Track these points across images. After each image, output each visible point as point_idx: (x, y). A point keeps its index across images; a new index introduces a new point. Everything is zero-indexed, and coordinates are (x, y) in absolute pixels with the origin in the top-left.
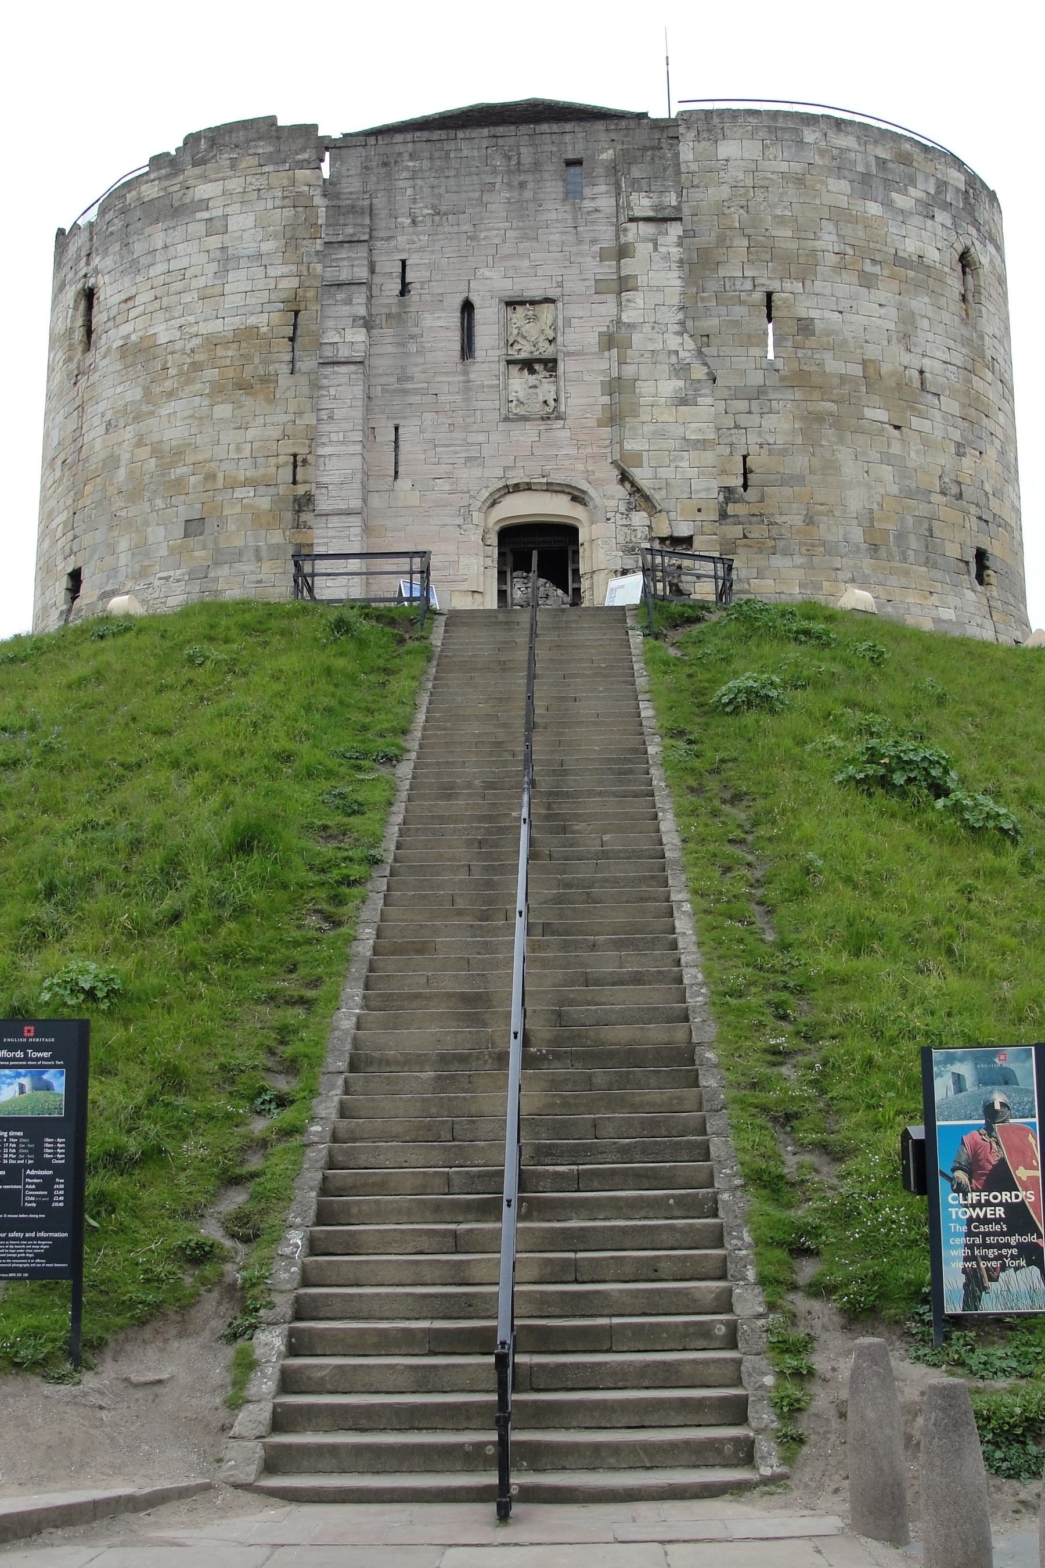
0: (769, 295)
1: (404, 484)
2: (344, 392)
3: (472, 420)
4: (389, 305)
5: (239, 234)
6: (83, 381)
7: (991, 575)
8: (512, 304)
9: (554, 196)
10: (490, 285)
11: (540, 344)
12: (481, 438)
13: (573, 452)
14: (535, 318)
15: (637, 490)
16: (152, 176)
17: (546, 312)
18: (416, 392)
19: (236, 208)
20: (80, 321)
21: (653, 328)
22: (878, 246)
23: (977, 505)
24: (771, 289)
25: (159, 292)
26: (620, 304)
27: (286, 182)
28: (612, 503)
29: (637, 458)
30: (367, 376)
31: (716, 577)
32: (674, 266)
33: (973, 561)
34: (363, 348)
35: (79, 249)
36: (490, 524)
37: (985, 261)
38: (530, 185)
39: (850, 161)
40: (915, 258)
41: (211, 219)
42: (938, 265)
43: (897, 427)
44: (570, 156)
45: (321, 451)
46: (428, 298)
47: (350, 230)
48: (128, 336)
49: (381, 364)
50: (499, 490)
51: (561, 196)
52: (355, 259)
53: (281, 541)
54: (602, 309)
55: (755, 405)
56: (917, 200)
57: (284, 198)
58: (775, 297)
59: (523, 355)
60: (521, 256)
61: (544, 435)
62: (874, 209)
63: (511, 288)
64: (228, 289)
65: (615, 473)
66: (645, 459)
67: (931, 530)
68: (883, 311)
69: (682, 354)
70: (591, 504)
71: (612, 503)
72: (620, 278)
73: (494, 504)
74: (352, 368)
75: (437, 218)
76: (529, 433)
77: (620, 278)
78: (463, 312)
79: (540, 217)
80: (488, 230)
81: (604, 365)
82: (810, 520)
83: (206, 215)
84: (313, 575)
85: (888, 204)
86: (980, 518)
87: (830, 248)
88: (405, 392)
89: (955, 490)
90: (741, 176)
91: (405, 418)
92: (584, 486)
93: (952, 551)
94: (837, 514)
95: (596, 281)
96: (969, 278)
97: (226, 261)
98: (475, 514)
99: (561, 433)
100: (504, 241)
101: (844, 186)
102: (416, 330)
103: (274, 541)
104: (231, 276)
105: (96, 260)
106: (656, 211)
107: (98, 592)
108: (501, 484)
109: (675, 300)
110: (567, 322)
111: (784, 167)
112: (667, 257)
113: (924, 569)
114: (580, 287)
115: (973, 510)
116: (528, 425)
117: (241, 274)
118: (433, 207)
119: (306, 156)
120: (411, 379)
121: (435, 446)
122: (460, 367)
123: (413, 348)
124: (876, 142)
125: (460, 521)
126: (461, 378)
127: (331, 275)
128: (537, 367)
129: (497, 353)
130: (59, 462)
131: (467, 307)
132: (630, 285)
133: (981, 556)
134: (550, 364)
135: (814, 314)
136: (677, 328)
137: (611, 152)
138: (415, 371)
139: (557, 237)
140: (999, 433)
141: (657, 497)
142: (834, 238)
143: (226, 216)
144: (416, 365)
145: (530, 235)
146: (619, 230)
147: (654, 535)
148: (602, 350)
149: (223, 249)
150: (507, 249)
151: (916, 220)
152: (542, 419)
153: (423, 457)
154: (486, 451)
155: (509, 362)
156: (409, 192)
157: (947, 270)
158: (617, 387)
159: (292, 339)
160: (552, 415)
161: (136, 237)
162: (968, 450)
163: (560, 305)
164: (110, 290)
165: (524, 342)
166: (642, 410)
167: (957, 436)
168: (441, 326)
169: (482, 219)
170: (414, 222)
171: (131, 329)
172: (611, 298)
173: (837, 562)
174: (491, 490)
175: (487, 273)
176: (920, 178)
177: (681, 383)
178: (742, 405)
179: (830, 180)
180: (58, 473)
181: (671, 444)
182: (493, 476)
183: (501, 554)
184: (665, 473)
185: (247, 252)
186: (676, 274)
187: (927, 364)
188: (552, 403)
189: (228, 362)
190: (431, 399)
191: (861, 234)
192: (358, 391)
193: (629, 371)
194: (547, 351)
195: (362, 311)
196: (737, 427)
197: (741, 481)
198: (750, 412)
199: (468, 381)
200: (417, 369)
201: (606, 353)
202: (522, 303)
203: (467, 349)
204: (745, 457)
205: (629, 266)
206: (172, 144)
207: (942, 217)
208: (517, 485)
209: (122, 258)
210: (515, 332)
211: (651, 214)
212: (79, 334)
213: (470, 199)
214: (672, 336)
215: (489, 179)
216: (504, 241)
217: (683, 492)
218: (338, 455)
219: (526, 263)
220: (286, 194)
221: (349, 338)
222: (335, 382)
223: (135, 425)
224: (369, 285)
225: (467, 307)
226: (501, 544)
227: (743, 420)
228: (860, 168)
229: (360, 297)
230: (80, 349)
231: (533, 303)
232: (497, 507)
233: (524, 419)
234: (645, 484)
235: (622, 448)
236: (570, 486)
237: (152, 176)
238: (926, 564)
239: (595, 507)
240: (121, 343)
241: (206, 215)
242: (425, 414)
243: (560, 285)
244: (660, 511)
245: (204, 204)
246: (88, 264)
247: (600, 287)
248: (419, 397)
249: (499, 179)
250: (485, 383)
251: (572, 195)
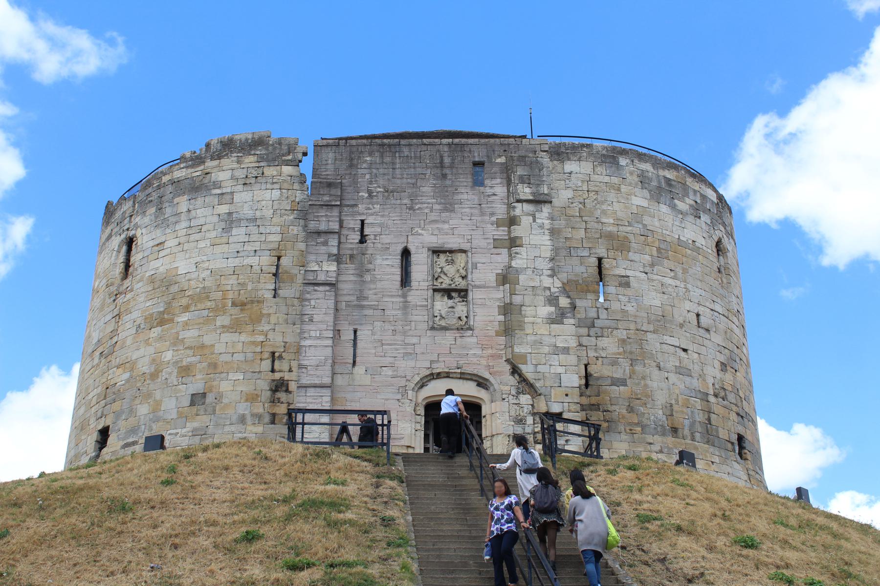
0: (600, 260)
1: (359, 370)
2: (321, 305)
3: (408, 328)
4: (352, 249)
5: (240, 205)
6: (121, 299)
8: (436, 252)
9: (465, 184)
11: (456, 280)
12: (415, 340)
13: (479, 352)
14: (452, 262)
15: (523, 380)
16: (182, 166)
17: (460, 259)
18: (370, 307)
19: (240, 187)
20: (122, 258)
21: (533, 272)
22: (668, 233)
23: (736, 405)
24: (601, 255)
25: (182, 240)
26: (510, 255)
27: (275, 173)
28: (507, 388)
29: (523, 358)
30: (336, 295)
31: (589, 437)
32: (547, 232)
33: (736, 442)
34: (335, 275)
35: (124, 212)
36: (420, 400)
37: (730, 248)
38: (449, 177)
39: (648, 179)
40: (690, 242)
41: (223, 194)
42: (705, 248)
43: (685, 350)
44: (477, 159)
45: (303, 343)
46: (379, 246)
47: (326, 198)
48: (157, 269)
49: (346, 287)
50: (426, 376)
51: (470, 184)
52: (331, 216)
53: (261, 410)
54: (498, 258)
55: (593, 331)
56: (691, 206)
57: (273, 183)
58: (605, 261)
59: (444, 286)
60: (444, 222)
61: (459, 340)
62: (664, 208)
63: (434, 241)
64: (231, 240)
65: (508, 368)
66: (529, 359)
67: (709, 419)
68: (672, 274)
69: (553, 290)
70: (491, 389)
71: (507, 388)
72: (510, 239)
73: (422, 387)
74: (327, 288)
75: (386, 194)
77: (510, 239)
78: (402, 256)
79: (456, 197)
80: (422, 203)
81: (499, 294)
82: (631, 409)
83: (218, 191)
84: (303, 424)
85: (673, 207)
86: (738, 414)
87: (638, 232)
88: (362, 307)
89: (722, 394)
90: (580, 184)
91: (361, 324)
92: (486, 375)
94: (648, 406)
95: (494, 240)
96: (721, 258)
97: (230, 221)
98: (410, 392)
99: (470, 340)
100: (431, 211)
101: (646, 193)
102: (371, 266)
103: (256, 411)
104: (235, 231)
105: (137, 219)
106: (534, 196)
107: (122, 443)
108: (428, 372)
109: (548, 254)
110: (475, 266)
111: (607, 179)
112: (541, 226)
113: (706, 446)
114: (483, 243)
115: (734, 408)
116: (448, 333)
117: (243, 230)
118: (384, 187)
119: (290, 157)
120: (366, 298)
121: (383, 345)
122: (400, 292)
123: (368, 277)
124: (663, 168)
125: (399, 396)
126: (402, 300)
127: (312, 225)
128: (453, 294)
129: (427, 284)
130: (97, 353)
131: (406, 253)
132: (518, 243)
133: (740, 438)
134: (463, 293)
135: (629, 273)
136: (549, 272)
137: (504, 158)
138: (369, 293)
139: (468, 210)
140: (744, 359)
141: (538, 385)
142: (640, 226)
143: (232, 193)
144: (370, 289)
145: (449, 207)
146: (510, 207)
147: (535, 411)
148: (498, 285)
149: (230, 214)
150: (433, 218)
151: (691, 218)
152: (458, 329)
153: (374, 351)
154: (418, 351)
155: (435, 290)
156: (368, 176)
157: (710, 251)
158: (507, 309)
159: (275, 275)
160: (464, 327)
161: (167, 204)
162: (728, 368)
163: (470, 254)
164: (146, 238)
165: (445, 277)
166: (526, 326)
167: (722, 358)
168: (387, 267)
169: (417, 196)
170: (370, 195)
171: (160, 266)
172: (505, 251)
173: (650, 439)
174: (421, 376)
175: (420, 231)
176: (691, 194)
177: (553, 309)
178: (584, 331)
179: (636, 189)
180: (96, 361)
181: (546, 349)
182: (423, 367)
183: (427, 422)
184: (540, 368)
185: (246, 216)
186: (548, 238)
187: (701, 310)
188: (465, 319)
189: (229, 288)
190: (379, 312)
191: (657, 224)
192: (331, 303)
193: (517, 300)
194: (462, 284)
195: (335, 251)
196: (580, 345)
197: (583, 382)
198: (589, 336)
199: (406, 302)
200: (371, 292)
201: (501, 288)
202: (444, 252)
203: (405, 280)
204: (586, 366)
205: (517, 231)
206: (199, 147)
207: (705, 218)
208: (439, 374)
209: (156, 217)
210: (439, 270)
211: (531, 198)
212: (120, 267)
213: (408, 183)
214: (546, 278)
215: (419, 170)
216: (431, 211)
217: (555, 383)
218: (315, 346)
219: (446, 226)
220: (275, 181)
221: (325, 268)
222: (315, 296)
223: (159, 329)
224: (339, 233)
225: (406, 253)
226: (426, 415)
227: (585, 341)
228: (654, 183)
229: (333, 242)
231: (451, 252)
232: (425, 388)
233: (445, 329)
234: (530, 376)
235: (513, 351)
236: (477, 375)
237: (182, 166)
238: (708, 442)
239: (495, 390)
240: (153, 272)
241: (218, 191)
242: (376, 323)
243: (470, 241)
244: (540, 395)
245: (217, 185)
246: (130, 222)
247: (497, 243)
248: (371, 311)
249: (429, 171)
250: (418, 303)
251: (478, 182)
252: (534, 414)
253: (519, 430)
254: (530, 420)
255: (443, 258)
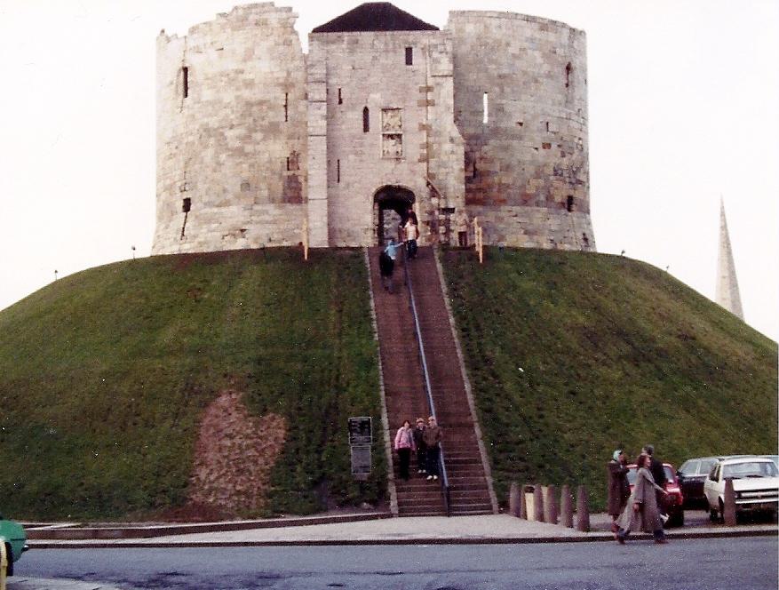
1: (342, 184)
7: (574, 207)
8: (385, 110)
10: (376, 100)
15: (433, 190)
43: (536, 149)
76: (390, 165)
93: (558, 199)
99: (404, 166)
131: (366, 110)
159: (286, 106)
172: (424, 109)
197: (472, 174)
203: (366, 128)
212: (181, 88)
225: (366, 110)
230: (182, 96)
252: (439, 209)
253: (430, 219)
254: (437, 213)
255: (390, 114)
